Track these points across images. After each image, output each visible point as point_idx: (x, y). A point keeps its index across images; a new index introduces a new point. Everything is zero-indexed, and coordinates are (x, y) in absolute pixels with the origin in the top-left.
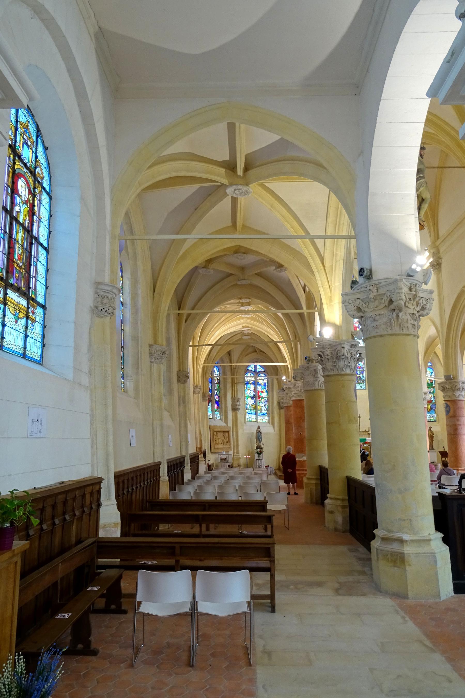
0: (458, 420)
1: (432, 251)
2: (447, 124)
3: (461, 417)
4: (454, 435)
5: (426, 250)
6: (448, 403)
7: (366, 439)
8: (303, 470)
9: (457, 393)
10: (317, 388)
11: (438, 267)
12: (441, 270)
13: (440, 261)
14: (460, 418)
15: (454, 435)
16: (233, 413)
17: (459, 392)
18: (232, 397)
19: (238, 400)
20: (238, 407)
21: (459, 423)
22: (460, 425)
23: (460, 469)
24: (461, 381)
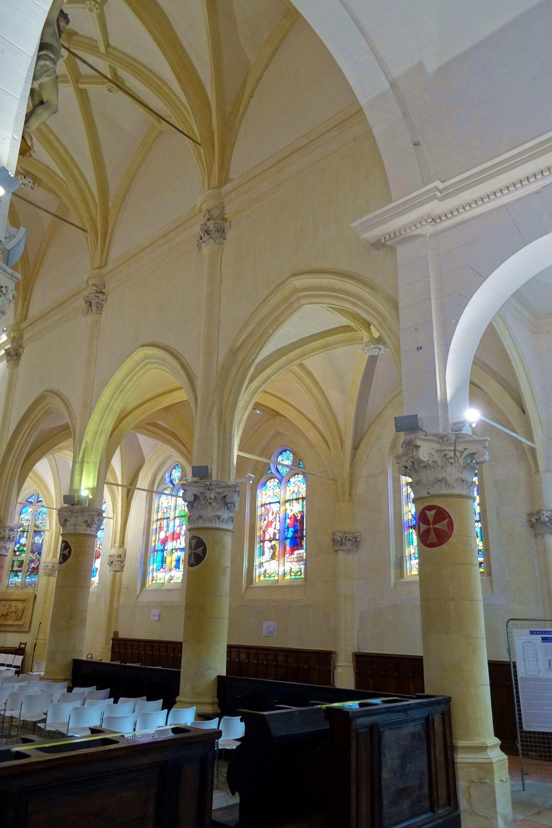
1: (12, 335)
2: (77, 166)
5: (4, 331)
11: (15, 357)
13: (21, 350)
24: (9, 527)
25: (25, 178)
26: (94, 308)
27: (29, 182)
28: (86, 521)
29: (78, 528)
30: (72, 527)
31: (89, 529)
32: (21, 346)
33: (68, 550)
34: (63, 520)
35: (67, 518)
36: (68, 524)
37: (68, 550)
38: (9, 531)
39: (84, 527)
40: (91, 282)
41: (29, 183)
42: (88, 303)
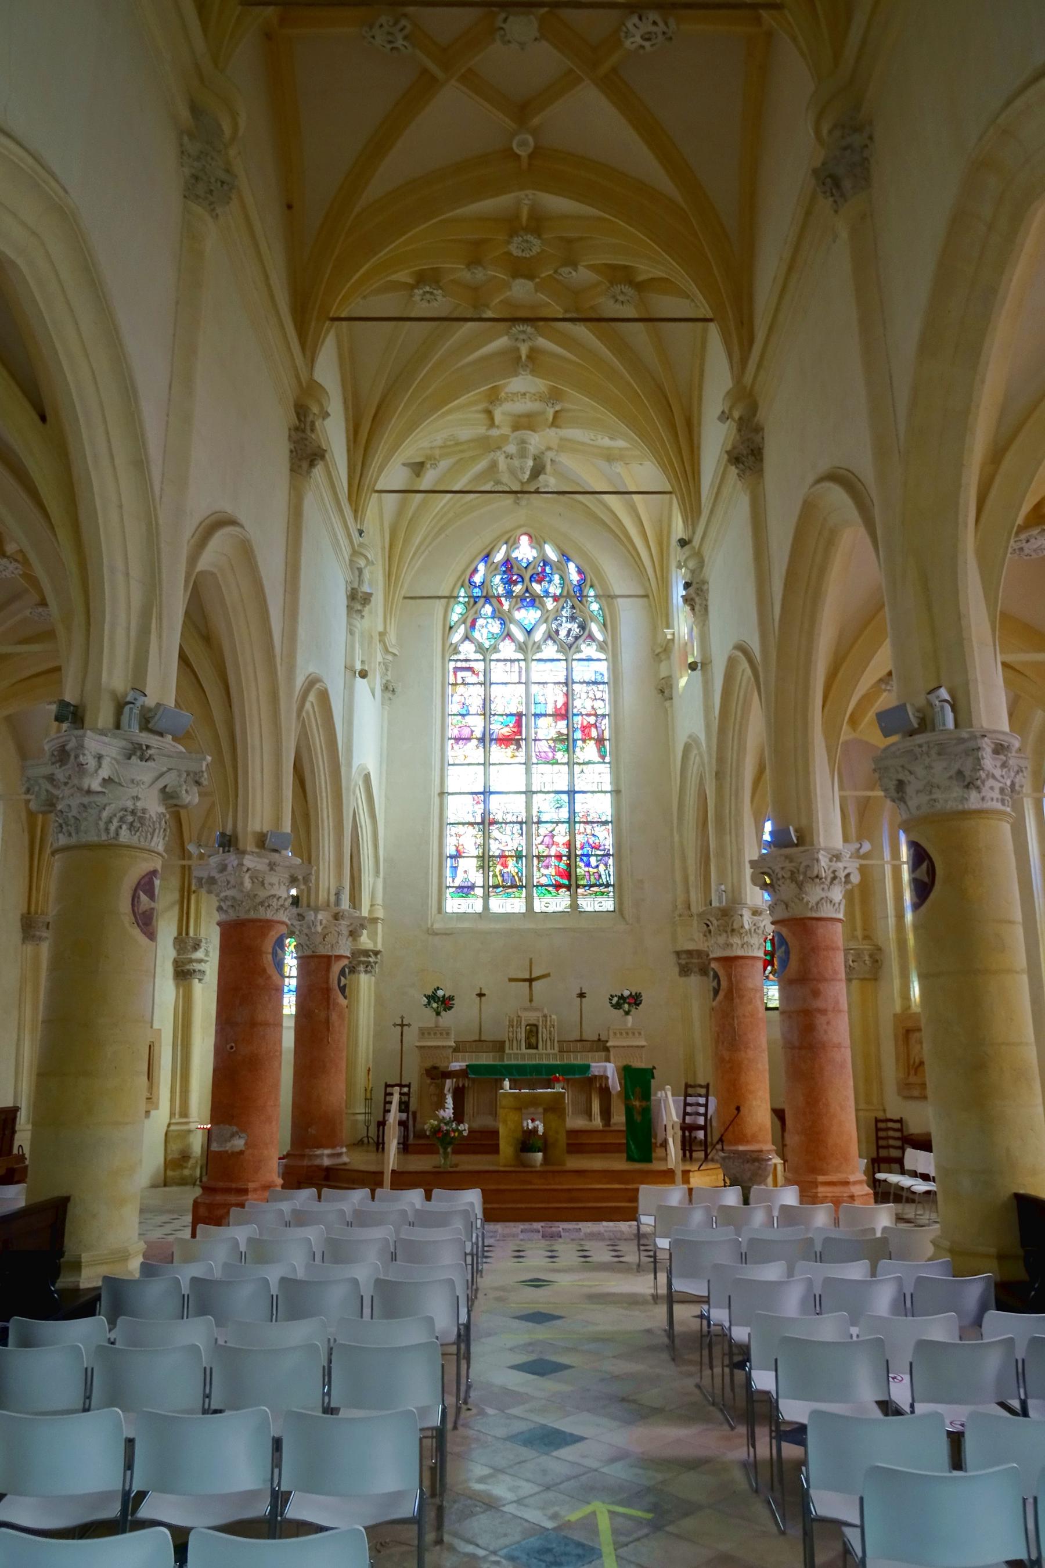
0: (816, 994)
3: (826, 980)
4: (800, 1048)
6: (784, 932)
7: (588, 1067)
8: (228, 1191)
9: (814, 894)
10: (92, 838)
11: (751, 458)
12: (761, 470)
14: (821, 987)
15: (800, 1048)
16: (177, 987)
17: (818, 889)
18: (180, 933)
19: (196, 947)
20: (197, 966)
21: (819, 1004)
22: (823, 1012)
23: (821, 1178)
24: (825, 849)
25: (640, 18)
26: (847, 184)
27: (655, 23)
28: (960, 773)
29: (937, 795)
30: (924, 798)
31: (974, 795)
32: (758, 429)
33: (924, 866)
34: (892, 785)
35: (901, 777)
36: (910, 790)
37: (924, 866)
38: (831, 860)
39: (957, 791)
40: (825, 131)
41: (654, 29)
42: (829, 180)
